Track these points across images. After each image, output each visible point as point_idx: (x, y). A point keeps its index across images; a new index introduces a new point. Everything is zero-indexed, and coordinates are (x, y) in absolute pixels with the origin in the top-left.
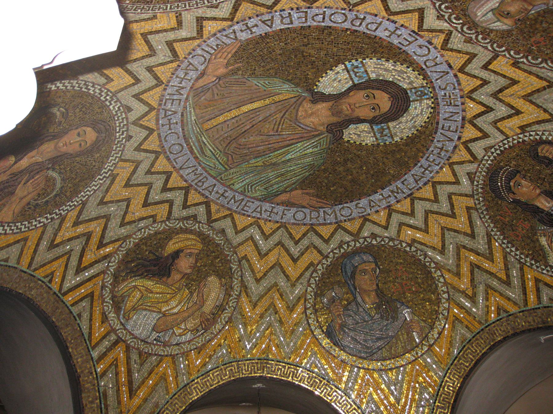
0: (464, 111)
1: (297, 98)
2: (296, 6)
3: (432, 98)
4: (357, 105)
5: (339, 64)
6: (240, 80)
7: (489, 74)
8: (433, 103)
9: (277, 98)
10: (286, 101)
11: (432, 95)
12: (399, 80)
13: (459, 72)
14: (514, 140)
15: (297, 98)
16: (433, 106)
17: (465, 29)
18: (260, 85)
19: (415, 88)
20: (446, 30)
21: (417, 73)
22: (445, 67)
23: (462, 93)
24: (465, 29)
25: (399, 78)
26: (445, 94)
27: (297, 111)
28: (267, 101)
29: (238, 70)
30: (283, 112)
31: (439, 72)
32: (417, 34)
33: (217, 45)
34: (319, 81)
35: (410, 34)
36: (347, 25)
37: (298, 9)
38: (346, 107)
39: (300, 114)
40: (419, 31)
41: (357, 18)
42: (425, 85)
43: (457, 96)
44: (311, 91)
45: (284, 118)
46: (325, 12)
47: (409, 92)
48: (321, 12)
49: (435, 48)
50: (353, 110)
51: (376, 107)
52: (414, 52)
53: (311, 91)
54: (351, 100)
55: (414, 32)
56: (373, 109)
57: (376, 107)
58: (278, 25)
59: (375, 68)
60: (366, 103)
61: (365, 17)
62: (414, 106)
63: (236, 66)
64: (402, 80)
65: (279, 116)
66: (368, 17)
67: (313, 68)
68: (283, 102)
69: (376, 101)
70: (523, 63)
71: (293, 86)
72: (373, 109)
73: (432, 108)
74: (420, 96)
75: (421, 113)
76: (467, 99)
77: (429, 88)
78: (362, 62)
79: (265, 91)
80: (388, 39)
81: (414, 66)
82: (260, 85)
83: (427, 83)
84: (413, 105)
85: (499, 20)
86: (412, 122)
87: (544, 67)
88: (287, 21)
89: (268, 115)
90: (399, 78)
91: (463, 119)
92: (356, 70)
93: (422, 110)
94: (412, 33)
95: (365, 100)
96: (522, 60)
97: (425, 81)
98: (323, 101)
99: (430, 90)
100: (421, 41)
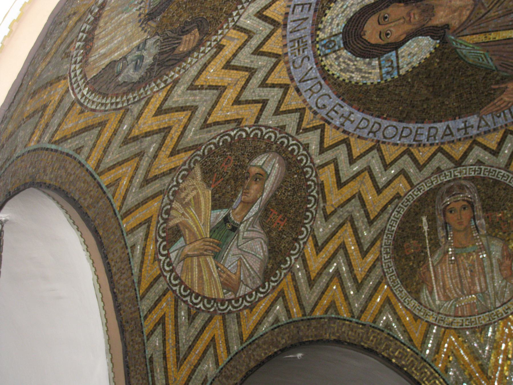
0: (284, 37)
1: (461, 34)
2: (420, 148)
3: (318, 42)
4: (402, 21)
5: (404, 75)
6: (504, 69)
7: (260, 96)
8: (318, 36)
9: (481, 38)
10: (475, 31)
11: (318, 46)
12: (349, 59)
13: (288, 85)
14: (228, 28)
15: (461, 34)
16: (318, 32)
17: (286, 141)
18: (489, 59)
19: (335, 52)
20: (302, 133)
21: (330, 73)
22: (303, 87)
23: (286, 58)
24: (286, 141)
25: (349, 62)
26: (303, 52)
27: (469, 17)
28: (492, 36)
29: (498, 81)
30: (484, 18)
31: (308, 80)
32: (326, 121)
33: (499, 117)
34: (431, 53)
35: (332, 119)
36: (385, 123)
37: (419, 145)
38: (414, 18)
39: (468, 13)
40: (324, 125)
41: (374, 133)
42: (324, 59)
43: (292, 54)
44: (444, 41)
45: (488, 9)
46: (399, 140)
47: (342, 46)
48: (402, 139)
49: (311, 108)
50: (409, 14)
51: (381, 21)
52: (330, 98)
53: (444, 41)
54: (408, 28)
55: (329, 123)
56: (386, 18)
57: (381, 21)
58: (441, 126)
59: (370, 73)
60: (390, 25)
61: (368, 134)
62: (340, 27)
63: (497, 87)
64: (346, 60)
65: (492, 14)
66: (365, 136)
67: (431, 70)
68: (478, 31)
69: (380, 28)
70: (233, 130)
71: (458, 50)
72: (386, 18)
73: (319, 29)
74: (330, 42)
75: (333, 19)
76: (281, 53)
77: (320, 55)
78: (382, 79)
79: (488, 51)
80: (353, 110)
81: (332, 80)
82: (489, 59)
83: (322, 61)
84: (340, 29)
85: (261, 167)
86: (345, 7)
87: (215, 138)
88: (433, 131)
89: (502, 18)
90: (349, 62)
91: (285, 25)
92: (390, 69)
93: (331, 24)
94: (331, 121)
95: (392, 29)
96: (235, 132)
97: (323, 63)
98: (437, 27)
99: (319, 52)
100: (323, 113)
